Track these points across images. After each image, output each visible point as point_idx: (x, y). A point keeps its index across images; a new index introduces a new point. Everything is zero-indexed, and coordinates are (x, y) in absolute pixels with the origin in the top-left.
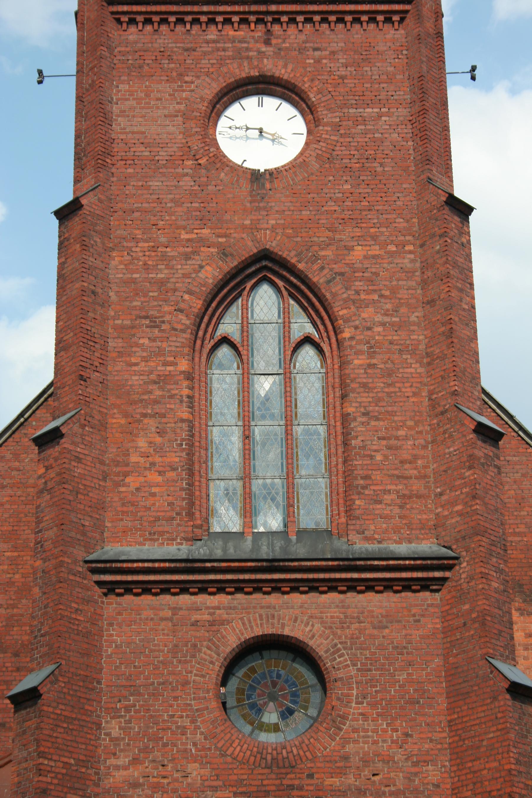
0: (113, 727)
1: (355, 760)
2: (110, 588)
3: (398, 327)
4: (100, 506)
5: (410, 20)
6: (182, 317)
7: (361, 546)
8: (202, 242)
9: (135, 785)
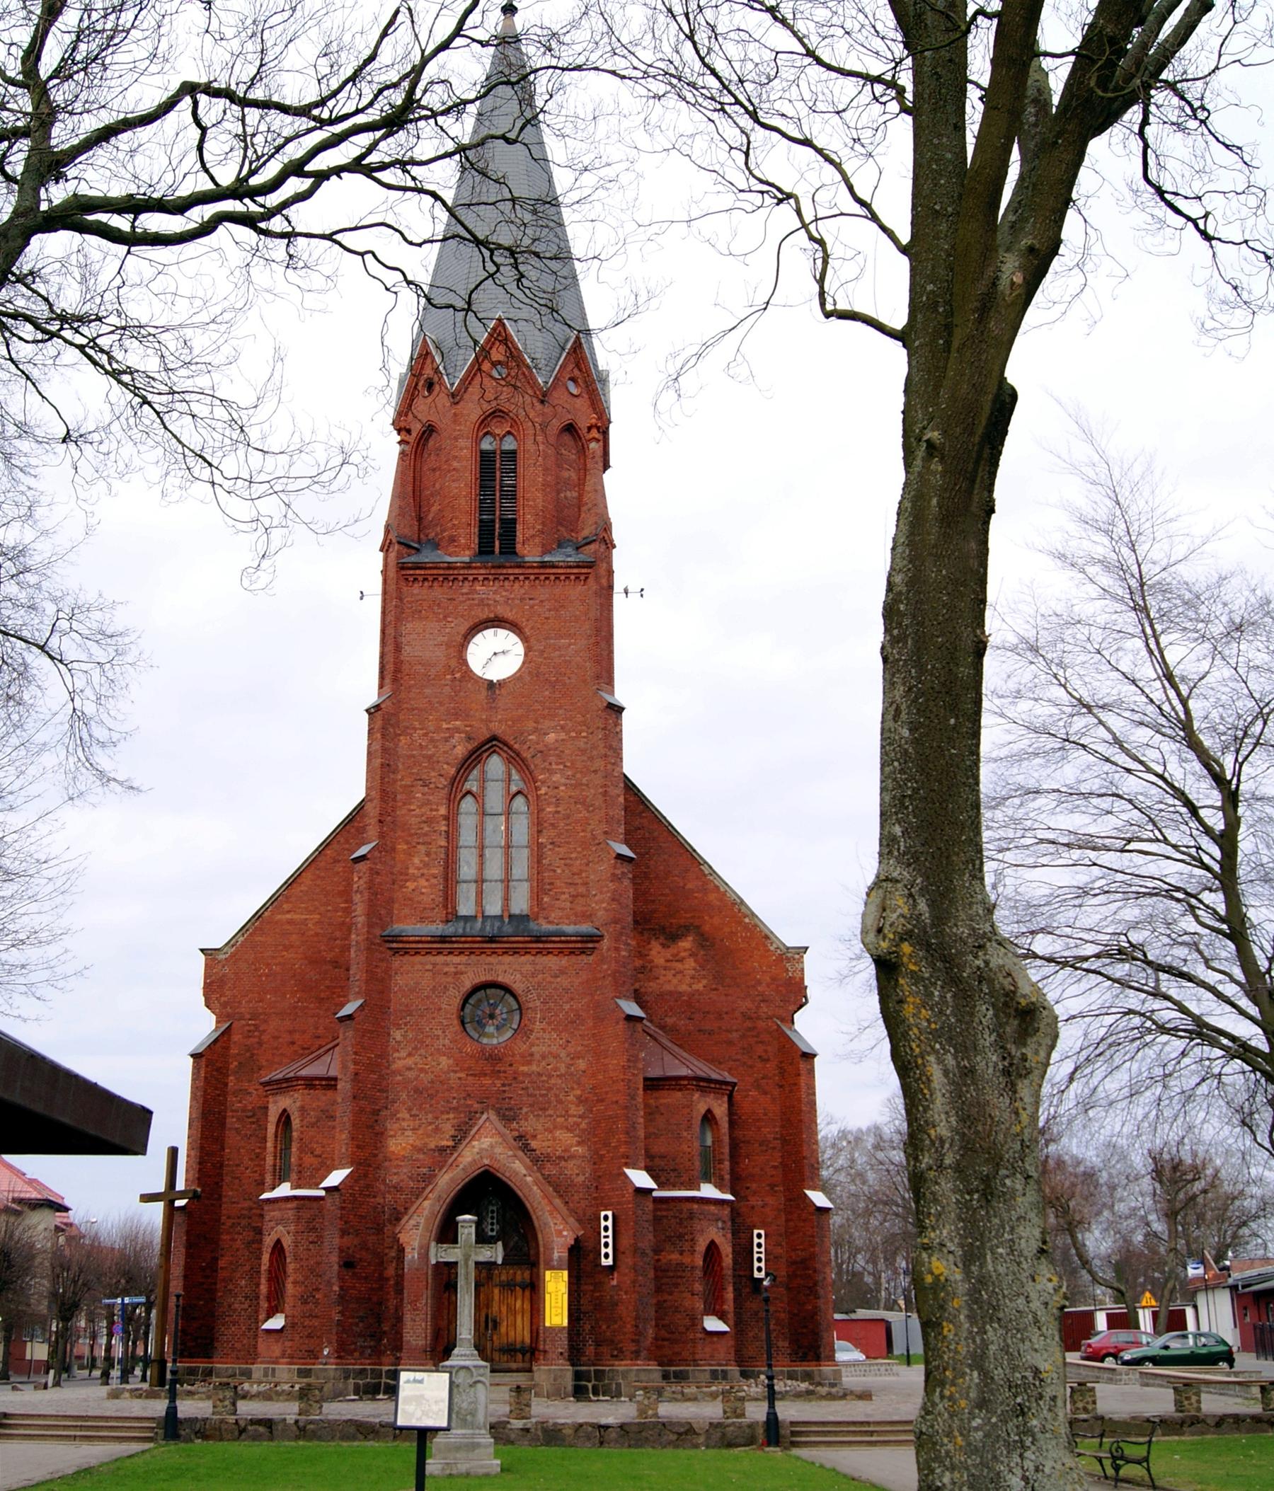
0: (398, 1035)
1: (537, 1056)
2: (396, 952)
3: (575, 786)
4: (391, 901)
5: (591, 580)
6: (442, 779)
7: (546, 927)
8: (458, 730)
9: (409, 1069)
